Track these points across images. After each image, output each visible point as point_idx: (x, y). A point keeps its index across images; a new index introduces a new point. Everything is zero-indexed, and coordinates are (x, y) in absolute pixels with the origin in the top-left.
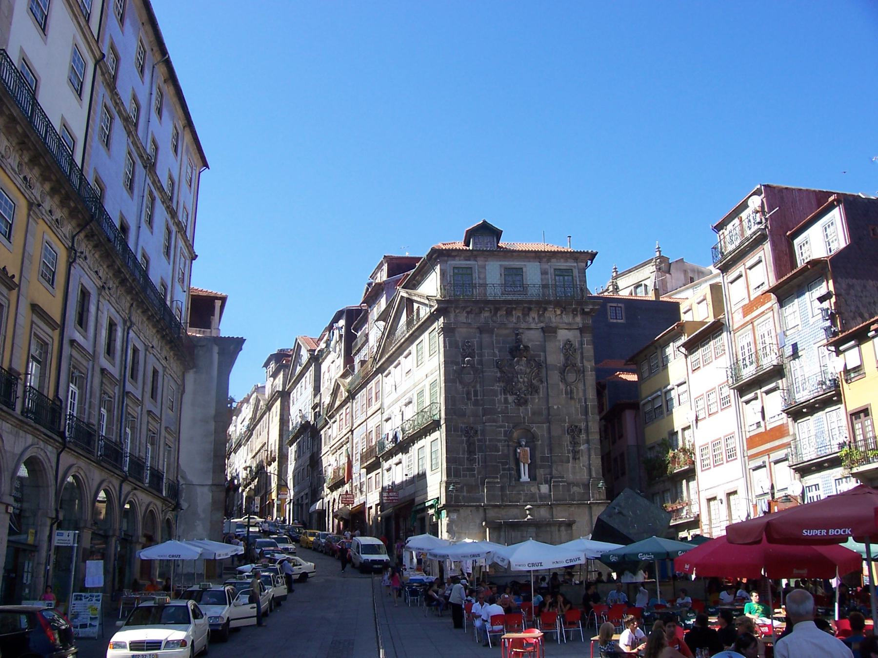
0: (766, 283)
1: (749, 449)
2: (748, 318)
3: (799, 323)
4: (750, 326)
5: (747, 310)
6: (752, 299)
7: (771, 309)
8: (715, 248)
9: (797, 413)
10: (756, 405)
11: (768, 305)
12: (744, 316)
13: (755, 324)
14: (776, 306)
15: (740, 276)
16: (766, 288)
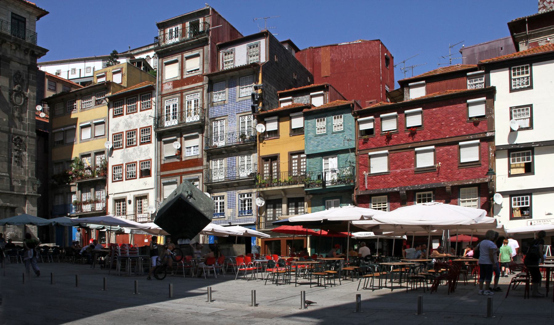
0: (201, 70)
1: (162, 171)
2: (178, 89)
3: (227, 99)
4: (179, 95)
5: (176, 83)
6: (185, 77)
7: (202, 87)
8: (157, 38)
9: (213, 153)
10: (176, 145)
11: (200, 84)
12: (174, 87)
13: (184, 94)
14: (206, 87)
15: (176, 61)
16: (199, 73)
